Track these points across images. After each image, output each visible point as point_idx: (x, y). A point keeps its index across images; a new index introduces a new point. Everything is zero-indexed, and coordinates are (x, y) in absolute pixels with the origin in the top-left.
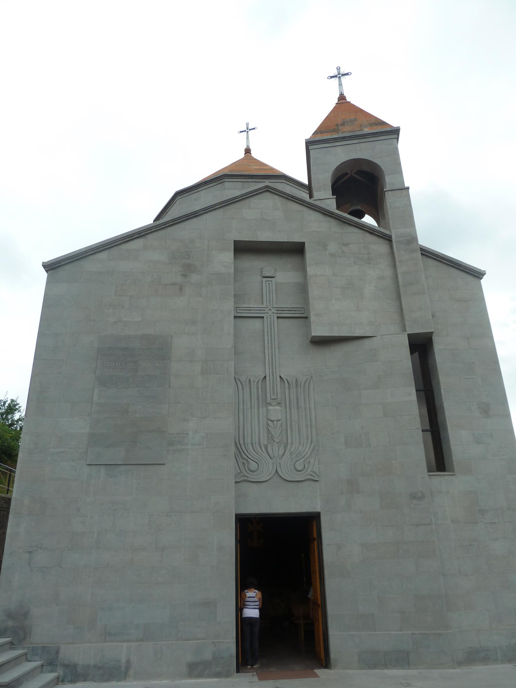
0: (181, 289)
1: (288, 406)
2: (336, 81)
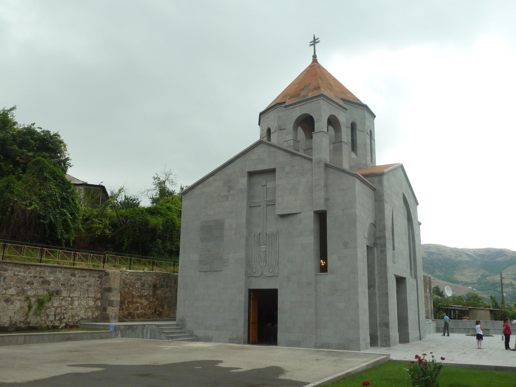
2: (312, 47)
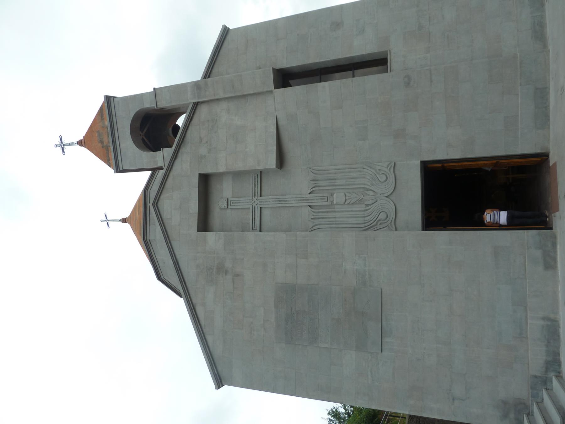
0: (238, 275)
1: (334, 188)
